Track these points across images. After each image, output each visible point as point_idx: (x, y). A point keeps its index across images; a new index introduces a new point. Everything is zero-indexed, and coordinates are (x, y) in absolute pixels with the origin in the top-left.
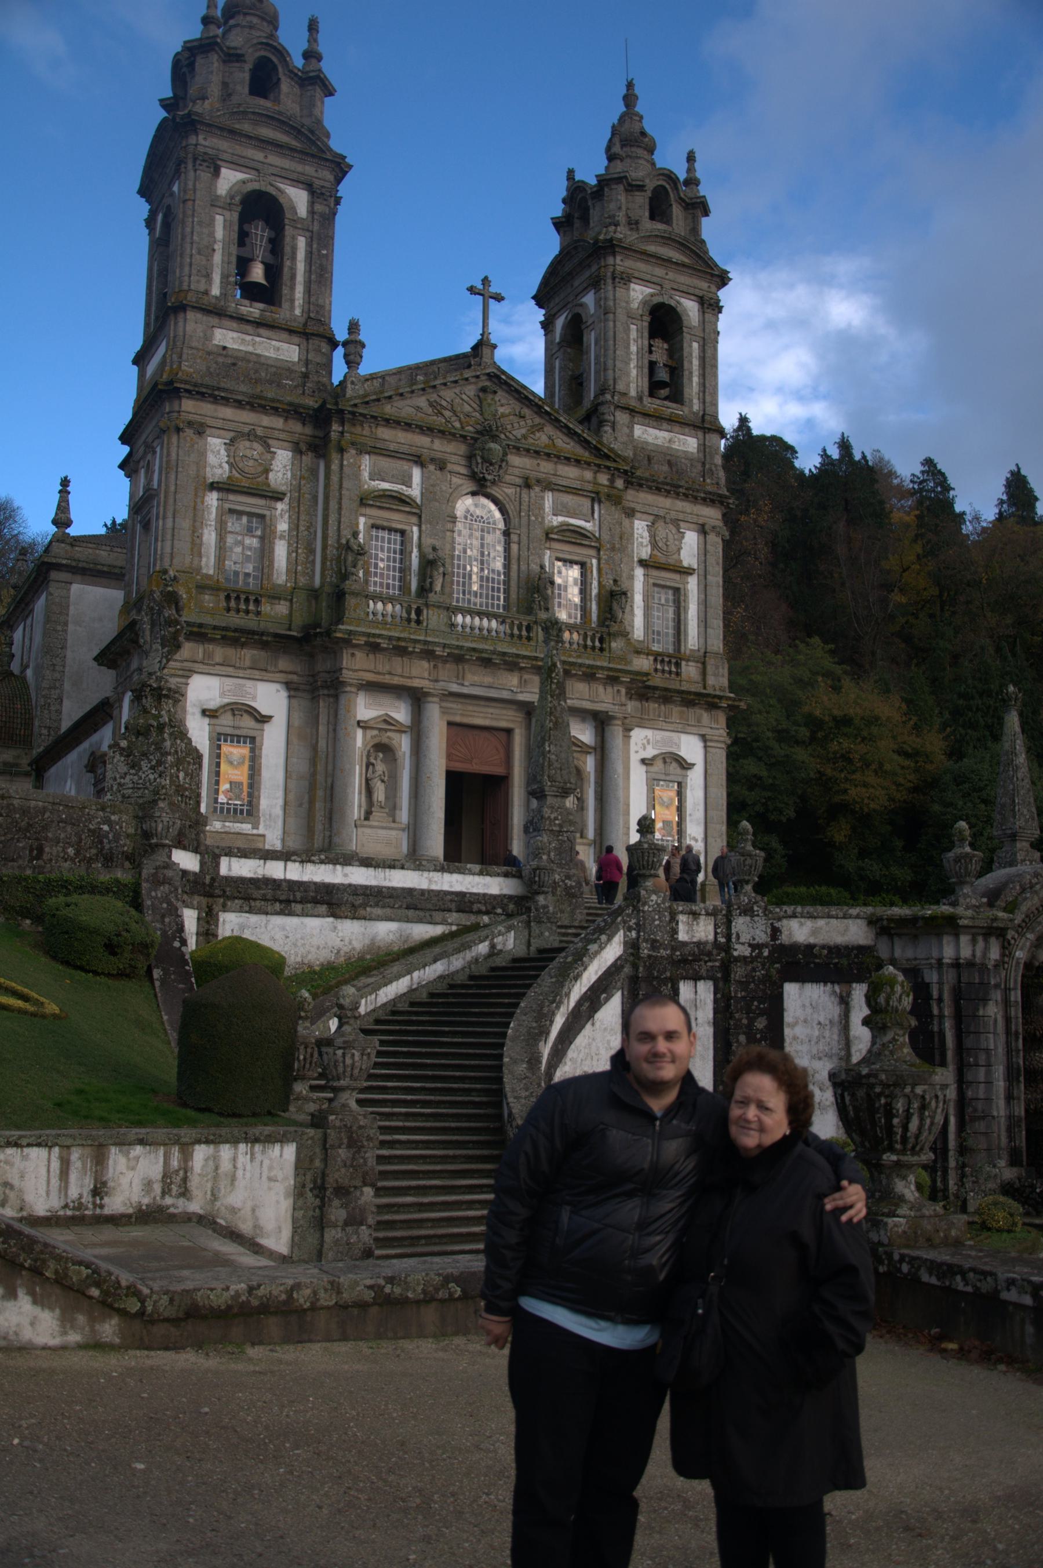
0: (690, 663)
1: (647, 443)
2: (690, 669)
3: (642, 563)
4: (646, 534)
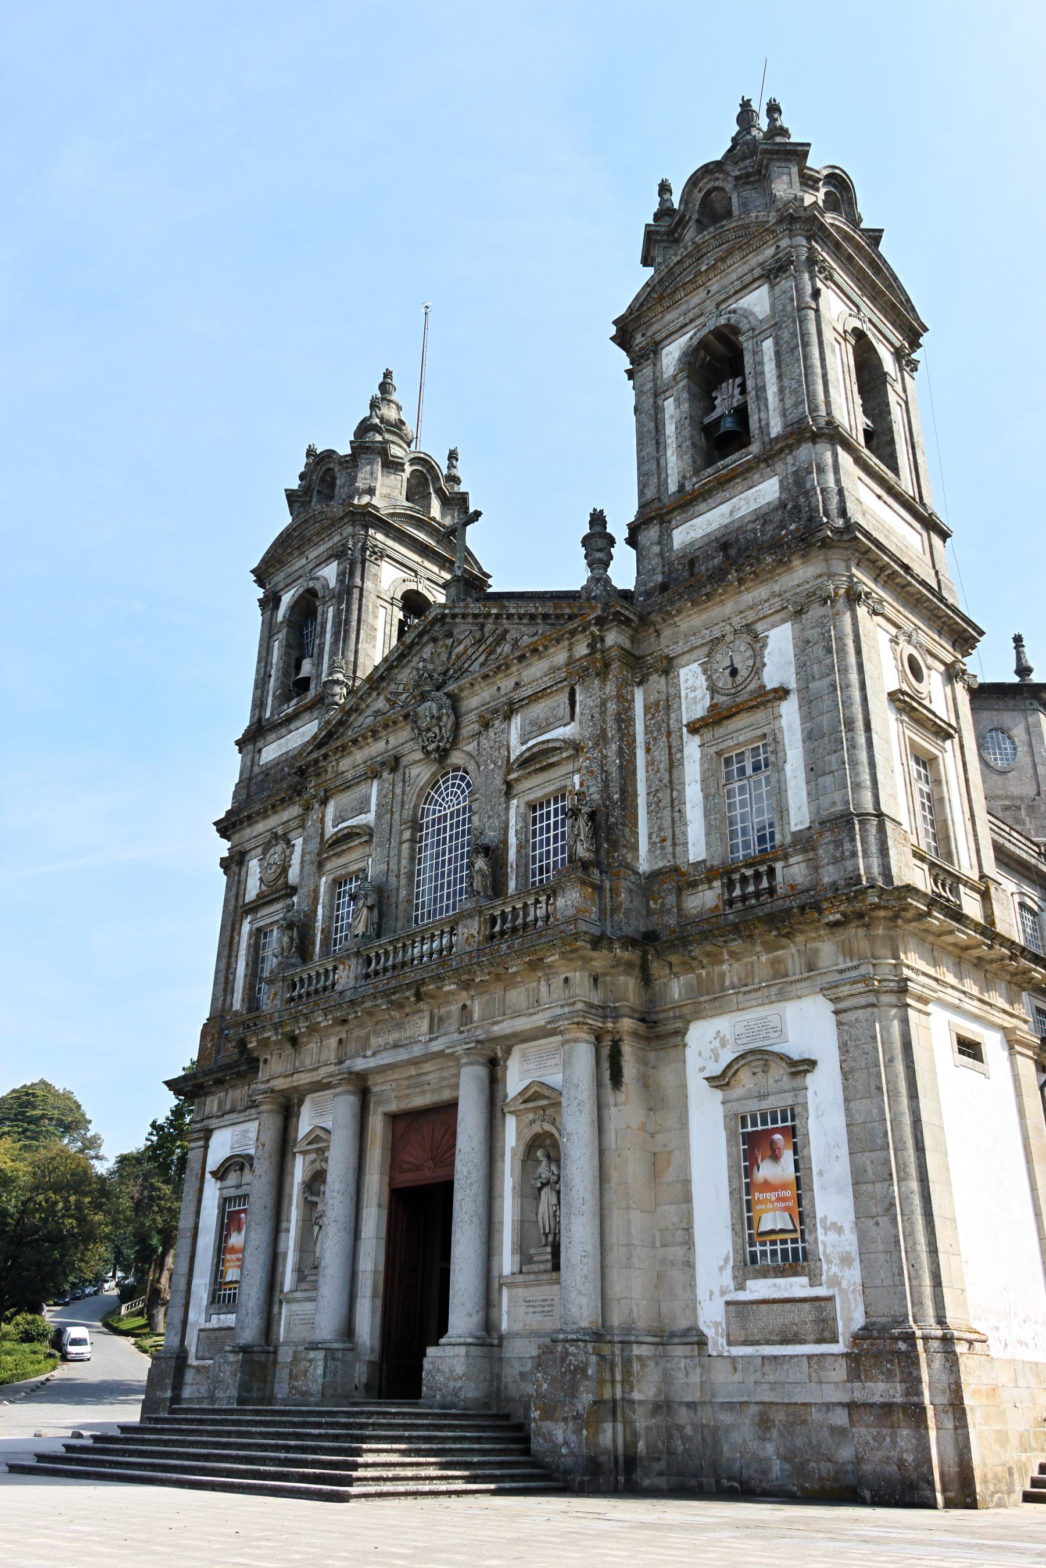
0: (792, 860)
1: (692, 543)
2: (796, 867)
3: (694, 728)
4: (702, 681)
